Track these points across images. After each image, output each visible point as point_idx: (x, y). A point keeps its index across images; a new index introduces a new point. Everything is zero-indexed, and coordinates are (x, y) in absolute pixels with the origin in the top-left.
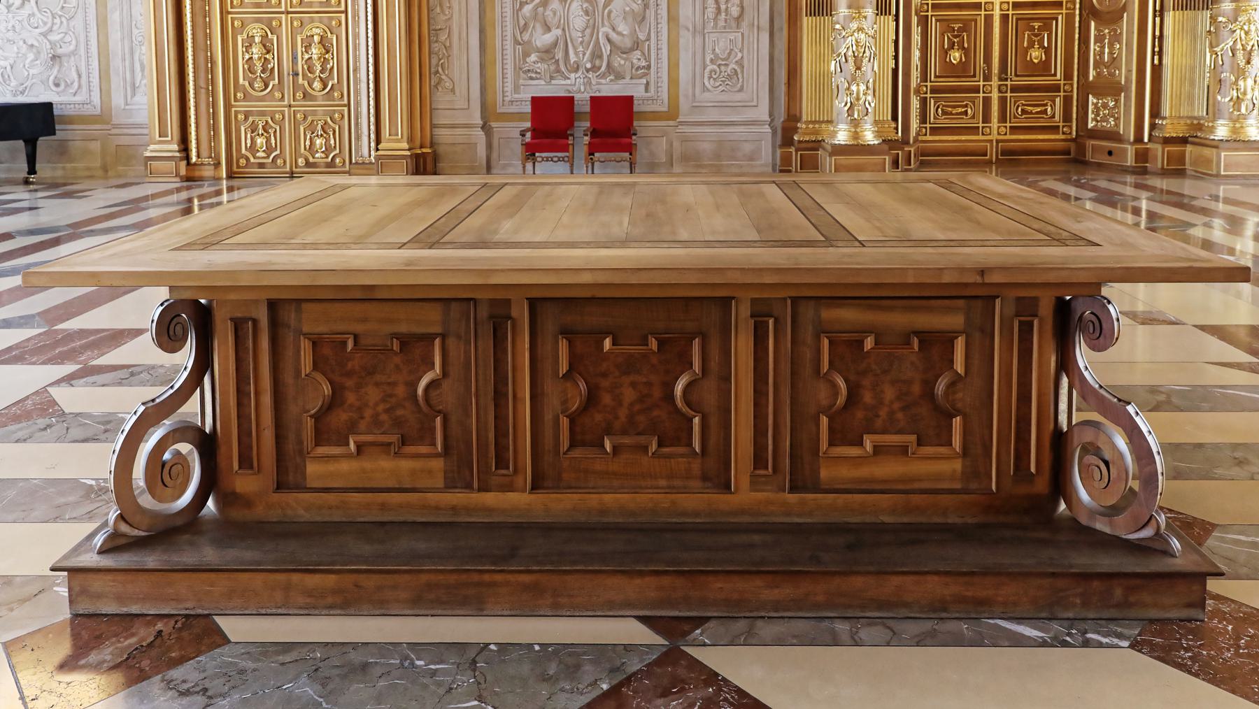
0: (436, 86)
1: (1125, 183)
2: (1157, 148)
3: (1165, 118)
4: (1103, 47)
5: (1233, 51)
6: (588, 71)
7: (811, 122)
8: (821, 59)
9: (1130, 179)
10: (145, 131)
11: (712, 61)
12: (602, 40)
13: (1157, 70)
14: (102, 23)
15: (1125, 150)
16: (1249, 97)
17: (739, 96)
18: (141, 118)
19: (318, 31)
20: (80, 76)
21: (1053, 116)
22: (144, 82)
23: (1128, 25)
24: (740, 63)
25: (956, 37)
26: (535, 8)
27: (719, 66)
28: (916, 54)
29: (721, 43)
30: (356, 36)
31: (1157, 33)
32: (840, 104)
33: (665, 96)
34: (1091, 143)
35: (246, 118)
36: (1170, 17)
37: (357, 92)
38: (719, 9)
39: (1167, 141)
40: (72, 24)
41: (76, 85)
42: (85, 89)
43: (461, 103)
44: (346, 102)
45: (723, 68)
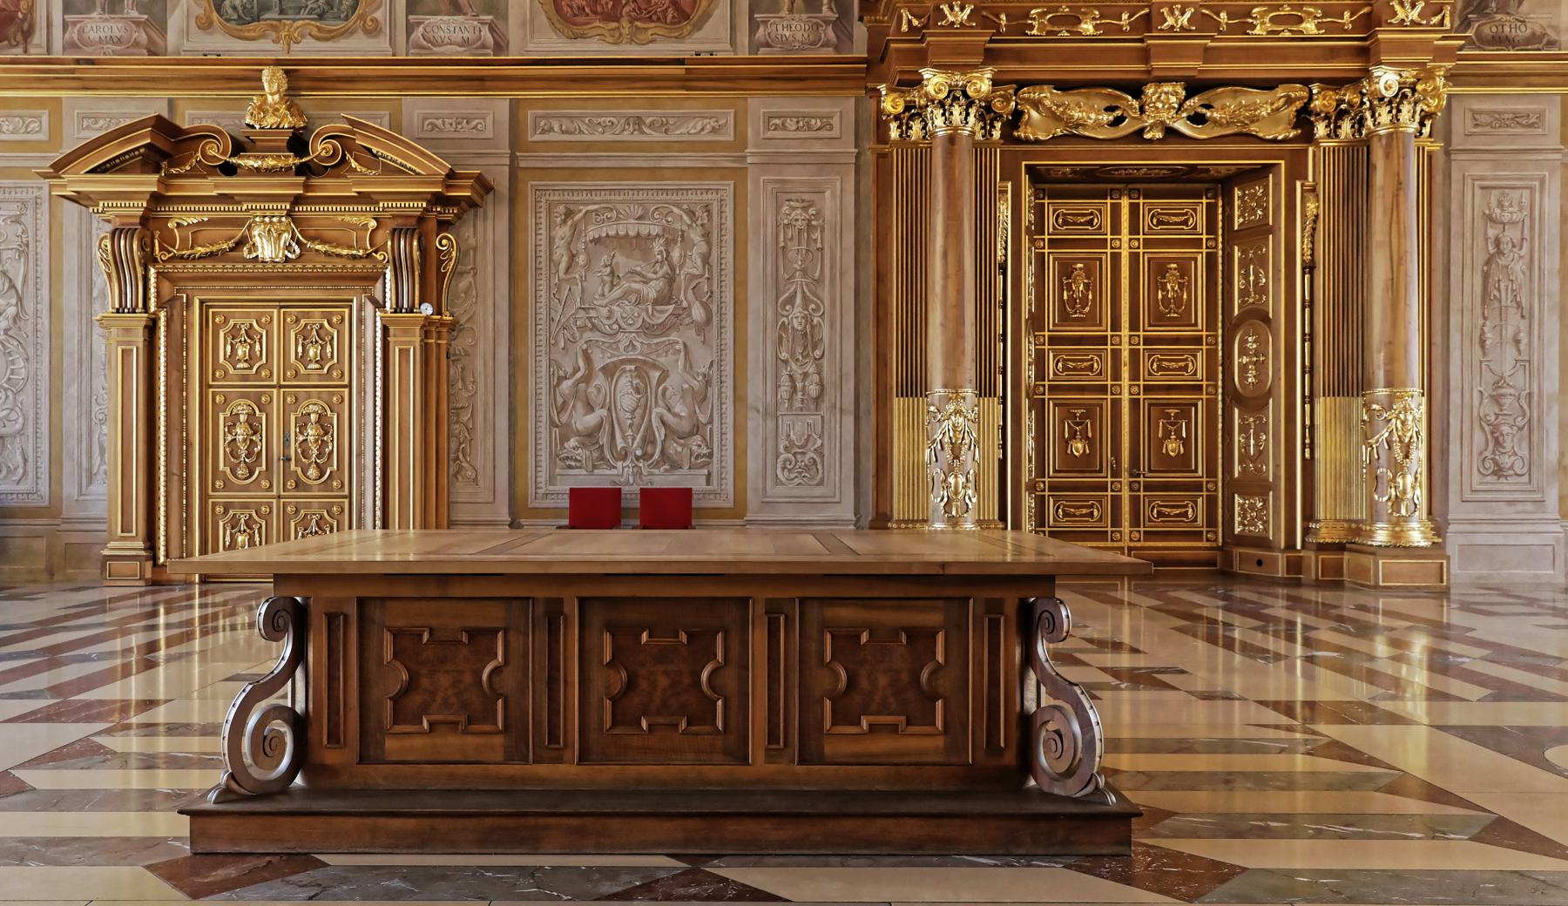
0: (455, 476)
1: (1276, 596)
2: (1310, 555)
3: (1318, 521)
4: (1248, 438)
5: (1389, 442)
6: (638, 458)
7: (904, 521)
8: (915, 447)
9: (1281, 591)
10: (104, 527)
11: (786, 448)
12: (655, 423)
13: (1309, 465)
14: (56, 397)
15: (1276, 558)
16: (1409, 496)
17: (818, 491)
18: (99, 510)
19: (316, 408)
20: (25, 461)
21: (1195, 520)
22: (104, 467)
23: (1274, 411)
24: (819, 451)
25: (1078, 424)
26: (576, 384)
27: (795, 454)
28: (1029, 443)
29: (794, 427)
30: (361, 414)
31: (1308, 422)
32: (937, 500)
33: (730, 488)
34: (1237, 551)
35: (226, 512)
36: (1321, 404)
37: (361, 481)
38: (794, 388)
39: (1322, 547)
40: (19, 398)
41: (20, 471)
42: (31, 475)
43: (485, 496)
44: (346, 492)
45: (799, 457)
